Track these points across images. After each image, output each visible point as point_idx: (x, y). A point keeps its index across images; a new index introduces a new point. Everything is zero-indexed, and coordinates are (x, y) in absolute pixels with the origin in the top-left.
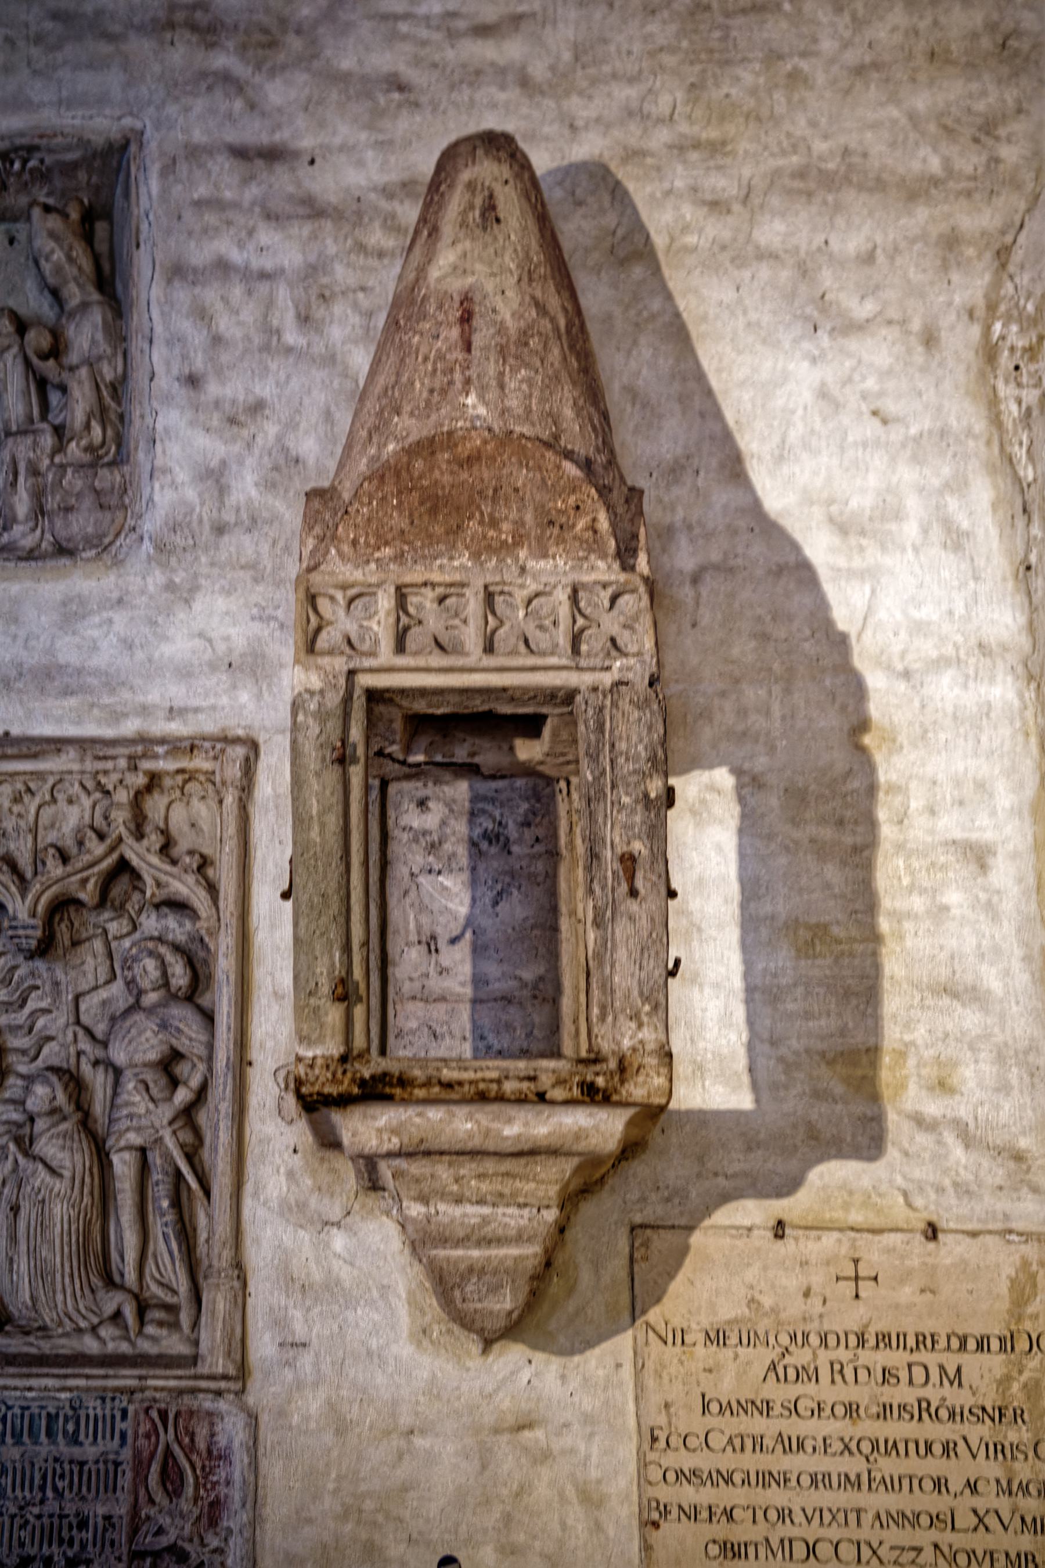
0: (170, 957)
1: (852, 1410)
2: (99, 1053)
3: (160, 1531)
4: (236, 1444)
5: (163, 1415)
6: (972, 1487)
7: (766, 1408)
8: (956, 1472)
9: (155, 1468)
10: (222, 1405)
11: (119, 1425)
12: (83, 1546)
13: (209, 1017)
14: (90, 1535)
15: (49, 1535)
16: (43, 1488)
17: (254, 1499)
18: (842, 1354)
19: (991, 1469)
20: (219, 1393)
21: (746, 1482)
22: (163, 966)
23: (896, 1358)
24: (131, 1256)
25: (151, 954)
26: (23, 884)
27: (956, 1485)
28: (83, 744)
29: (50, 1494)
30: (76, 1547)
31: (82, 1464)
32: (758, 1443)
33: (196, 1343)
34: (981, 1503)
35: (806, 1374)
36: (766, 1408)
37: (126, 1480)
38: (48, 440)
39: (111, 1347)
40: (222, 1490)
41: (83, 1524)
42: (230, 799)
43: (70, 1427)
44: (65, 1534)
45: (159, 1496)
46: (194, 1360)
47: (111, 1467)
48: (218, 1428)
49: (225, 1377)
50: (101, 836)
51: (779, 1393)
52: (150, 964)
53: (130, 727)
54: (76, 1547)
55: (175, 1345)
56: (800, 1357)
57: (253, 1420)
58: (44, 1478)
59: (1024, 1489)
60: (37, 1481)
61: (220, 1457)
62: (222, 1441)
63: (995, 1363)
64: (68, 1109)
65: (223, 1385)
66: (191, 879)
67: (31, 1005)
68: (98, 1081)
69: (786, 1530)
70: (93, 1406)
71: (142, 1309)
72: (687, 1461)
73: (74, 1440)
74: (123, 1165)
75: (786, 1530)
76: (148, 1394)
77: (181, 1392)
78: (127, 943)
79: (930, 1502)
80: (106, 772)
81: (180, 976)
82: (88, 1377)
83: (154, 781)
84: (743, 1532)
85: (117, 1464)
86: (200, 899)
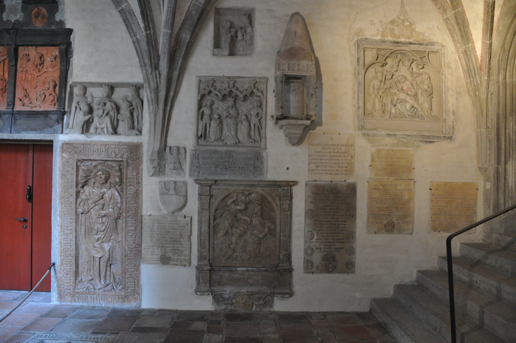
0: (258, 102)
1: (330, 152)
2: (249, 113)
5: (257, 153)
6: (342, 160)
7: (322, 152)
8: (340, 158)
9: (256, 158)
10: (264, 152)
13: (262, 109)
18: (330, 147)
19: (344, 158)
21: (319, 160)
22: (257, 103)
23: (335, 147)
24: (253, 135)
25: (256, 102)
26: (242, 93)
27: (340, 160)
28: (248, 77)
32: (321, 156)
33: (261, 145)
34: (343, 161)
35: (326, 149)
36: (322, 152)
38: (244, 42)
39: (251, 145)
42: (265, 85)
46: (260, 147)
49: (264, 149)
50: (250, 88)
51: (323, 151)
52: (256, 103)
53: (253, 76)
55: (258, 145)
56: (325, 147)
57: (267, 154)
59: (347, 160)
63: (345, 147)
64: (246, 119)
66: (261, 93)
67: (242, 107)
68: (249, 116)
69: (323, 165)
71: (255, 141)
72: (313, 158)
73: (247, 155)
74: (252, 125)
75: (323, 165)
78: (252, 100)
79: (338, 161)
80: (251, 81)
81: (259, 104)
83: (256, 82)
84: (318, 165)
86: (262, 96)
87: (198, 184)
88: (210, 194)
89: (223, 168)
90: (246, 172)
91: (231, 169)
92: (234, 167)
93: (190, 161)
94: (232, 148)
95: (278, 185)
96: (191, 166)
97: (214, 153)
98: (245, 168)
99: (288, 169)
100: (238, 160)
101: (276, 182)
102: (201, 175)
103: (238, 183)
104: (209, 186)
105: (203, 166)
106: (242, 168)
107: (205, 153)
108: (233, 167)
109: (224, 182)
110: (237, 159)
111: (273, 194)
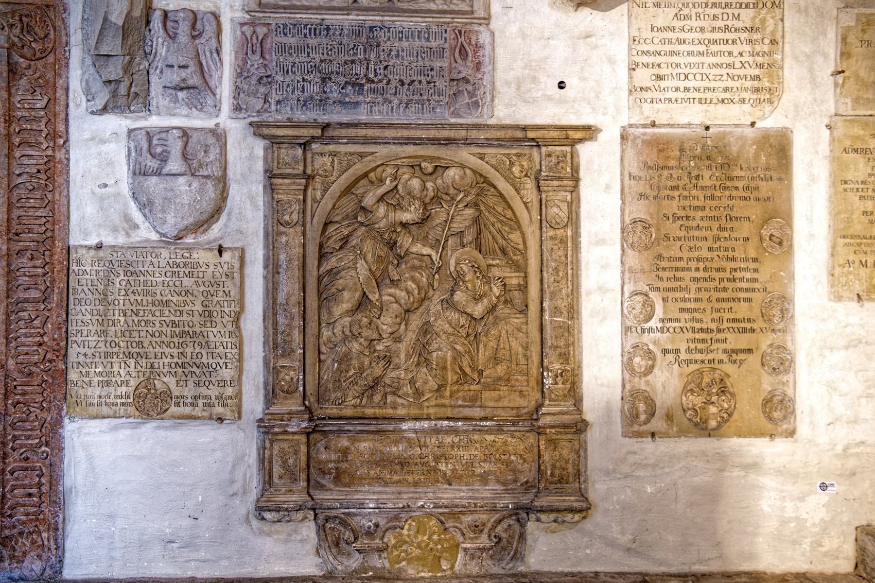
3: (459, 72)
4: (486, 42)
9: (457, 50)
10: (481, 29)
11: (444, 35)
12: (432, 77)
14: (435, 73)
15: (420, 73)
16: (417, 56)
17: (493, 61)
20: (480, 24)
29: (420, 58)
30: (430, 77)
31: (431, 49)
37: (447, 54)
39: (441, 7)
40: (481, 59)
41: (432, 70)
43: (426, 35)
44: (426, 73)
45: (459, 60)
46: (472, 12)
47: (442, 50)
48: (480, 37)
49: (484, 19)
54: (430, 77)
57: (493, 34)
58: (417, 53)
60: (415, 54)
61: (480, 47)
62: (481, 41)
65: (482, 21)
70: (434, 28)
73: (428, 40)
76: (454, 24)
77: (466, 24)
82: (433, 17)
85: (444, 49)
87: (264, 137)
88: (304, 172)
89: (346, 83)
90: (425, 97)
91: (373, 85)
92: (385, 82)
93: (236, 58)
94: (378, 18)
95: (533, 139)
96: (240, 75)
97: (315, 35)
98: (420, 82)
99: (561, 85)
100: (397, 56)
101: (524, 129)
102: (273, 108)
103: (399, 135)
104: (300, 144)
105: (279, 78)
106: (413, 81)
107: (285, 35)
108: (380, 81)
109: (352, 132)
110: (393, 53)
111: (514, 169)
